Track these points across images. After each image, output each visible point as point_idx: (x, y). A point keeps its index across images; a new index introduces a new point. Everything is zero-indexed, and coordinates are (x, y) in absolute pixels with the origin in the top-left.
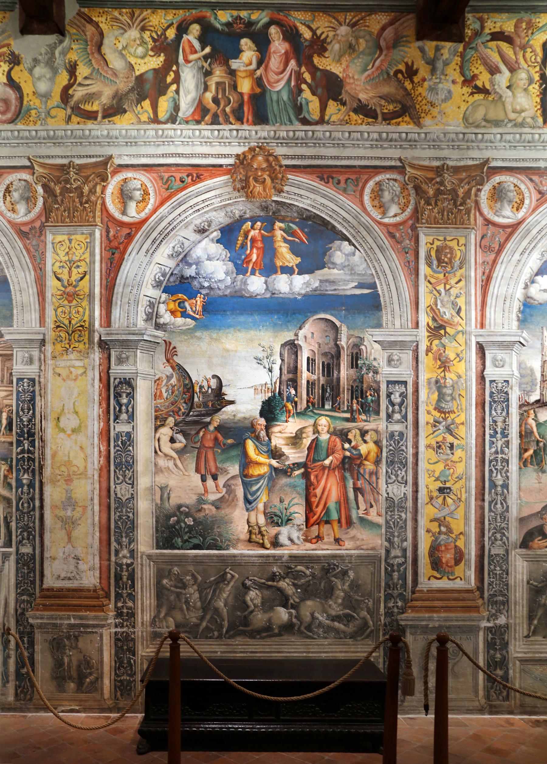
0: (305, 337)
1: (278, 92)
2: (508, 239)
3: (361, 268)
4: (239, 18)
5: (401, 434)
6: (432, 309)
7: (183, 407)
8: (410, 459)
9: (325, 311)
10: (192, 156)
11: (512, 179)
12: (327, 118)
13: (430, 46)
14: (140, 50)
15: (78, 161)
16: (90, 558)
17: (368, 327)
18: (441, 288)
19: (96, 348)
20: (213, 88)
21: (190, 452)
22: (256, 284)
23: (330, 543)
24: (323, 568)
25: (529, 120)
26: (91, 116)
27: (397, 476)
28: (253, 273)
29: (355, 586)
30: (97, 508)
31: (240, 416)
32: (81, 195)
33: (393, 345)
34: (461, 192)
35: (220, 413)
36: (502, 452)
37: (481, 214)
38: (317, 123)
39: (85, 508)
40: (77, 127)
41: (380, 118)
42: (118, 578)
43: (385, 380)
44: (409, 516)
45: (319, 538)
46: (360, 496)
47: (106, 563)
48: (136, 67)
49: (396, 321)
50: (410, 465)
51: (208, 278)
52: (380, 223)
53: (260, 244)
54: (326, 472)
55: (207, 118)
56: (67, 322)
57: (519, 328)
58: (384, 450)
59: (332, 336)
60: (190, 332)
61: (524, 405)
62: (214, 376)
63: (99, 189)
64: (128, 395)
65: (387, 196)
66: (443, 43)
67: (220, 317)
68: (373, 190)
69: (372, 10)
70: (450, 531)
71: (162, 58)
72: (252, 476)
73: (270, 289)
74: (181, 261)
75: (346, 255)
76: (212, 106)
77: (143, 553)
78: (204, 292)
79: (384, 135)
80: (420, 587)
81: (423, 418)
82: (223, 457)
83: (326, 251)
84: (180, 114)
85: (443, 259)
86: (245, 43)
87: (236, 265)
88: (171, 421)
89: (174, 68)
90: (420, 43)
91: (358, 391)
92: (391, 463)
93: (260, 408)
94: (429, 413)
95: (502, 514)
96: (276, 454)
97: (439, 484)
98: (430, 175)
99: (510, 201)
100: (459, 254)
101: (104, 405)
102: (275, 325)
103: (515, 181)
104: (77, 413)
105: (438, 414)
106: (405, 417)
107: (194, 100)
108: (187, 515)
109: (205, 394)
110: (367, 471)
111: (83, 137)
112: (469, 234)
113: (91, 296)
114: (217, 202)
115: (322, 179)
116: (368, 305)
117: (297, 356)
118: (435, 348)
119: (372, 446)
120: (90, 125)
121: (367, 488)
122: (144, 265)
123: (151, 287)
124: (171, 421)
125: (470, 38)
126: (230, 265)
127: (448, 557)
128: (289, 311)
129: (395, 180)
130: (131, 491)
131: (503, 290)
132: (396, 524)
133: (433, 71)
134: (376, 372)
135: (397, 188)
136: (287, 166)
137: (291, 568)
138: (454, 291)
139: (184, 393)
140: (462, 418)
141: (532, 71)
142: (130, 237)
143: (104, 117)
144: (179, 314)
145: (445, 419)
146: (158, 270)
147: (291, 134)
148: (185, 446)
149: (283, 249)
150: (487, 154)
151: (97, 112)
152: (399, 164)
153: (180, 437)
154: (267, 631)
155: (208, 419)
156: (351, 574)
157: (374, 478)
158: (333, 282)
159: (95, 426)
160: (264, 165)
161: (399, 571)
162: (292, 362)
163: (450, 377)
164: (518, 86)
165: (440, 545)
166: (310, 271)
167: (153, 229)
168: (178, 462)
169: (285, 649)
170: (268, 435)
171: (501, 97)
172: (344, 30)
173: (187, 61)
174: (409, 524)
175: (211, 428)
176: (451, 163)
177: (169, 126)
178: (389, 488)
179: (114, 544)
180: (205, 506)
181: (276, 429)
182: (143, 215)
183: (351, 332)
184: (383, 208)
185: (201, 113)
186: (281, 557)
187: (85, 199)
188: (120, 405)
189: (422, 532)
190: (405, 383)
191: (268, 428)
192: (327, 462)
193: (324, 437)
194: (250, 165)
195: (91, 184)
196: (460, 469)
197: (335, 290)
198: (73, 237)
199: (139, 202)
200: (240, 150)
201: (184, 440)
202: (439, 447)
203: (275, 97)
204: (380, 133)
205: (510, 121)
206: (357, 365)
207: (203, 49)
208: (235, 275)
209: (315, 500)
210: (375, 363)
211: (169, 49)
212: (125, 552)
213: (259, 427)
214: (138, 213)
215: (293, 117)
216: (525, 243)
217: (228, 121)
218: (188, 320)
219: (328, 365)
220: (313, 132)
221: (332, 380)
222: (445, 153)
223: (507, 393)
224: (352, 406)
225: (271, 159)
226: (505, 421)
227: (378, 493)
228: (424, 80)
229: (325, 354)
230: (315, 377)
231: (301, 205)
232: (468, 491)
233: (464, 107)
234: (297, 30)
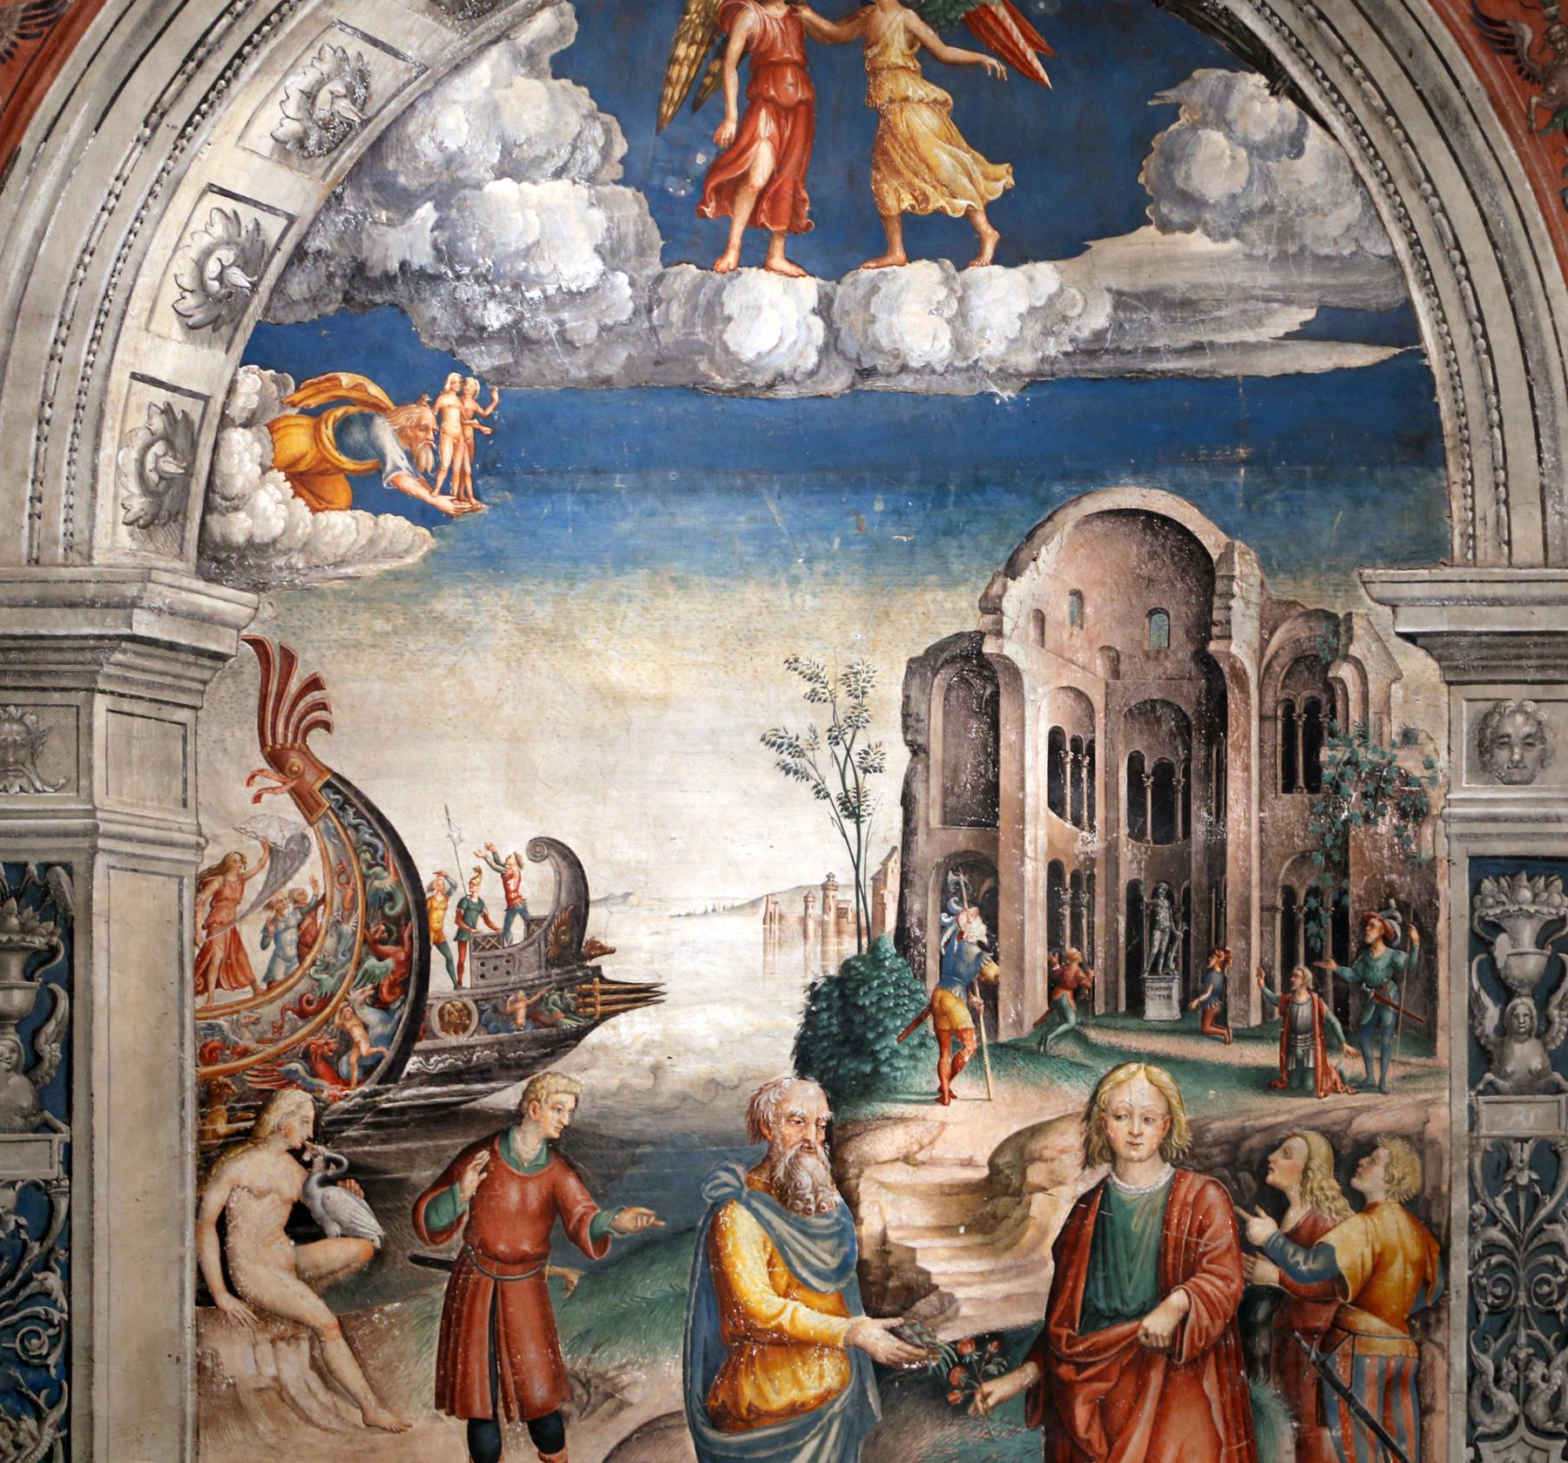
0: (1040, 618)
3: (1334, 223)
9: (1145, 470)
17: (1370, 559)
22: (772, 318)
27: (1524, 1393)
28: (754, 256)
31: (686, 1071)
35: (577, 1056)
43: (1460, 852)
51: (507, 282)
53: (790, 89)
54: (1156, 1379)
58: (1461, 1246)
59: (1179, 605)
62: (546, 847)
67: (570, 505)
72: (756, 1417)
73: (850, 346)
74: (354, 176)
75: (1258, 151)
78: (482, 359)
83: (1147, 128)
91: (1319, 922)
92: (1493, 1321)
96: (883, 1285)
102: (876, 551)
110: (1371, 1367)
117: (995, 726)
119: (1393, 1224)
122: (134, 197)
123: (176, 331)
126: (631, 206)
128: (942, 469)
134: (1415, 812)
144: (343, 493)
146: (219, 230)
149: (920, 115)
157: (1405, 1411)
158: (1184, 306)
162: (969, 758)
166: (1063, 245)
170: (840, 1180)
175: (527, 1144)
181: (883, 1144)
191: (837, 1139)
192: (1159, 1323)
193: (1144, 1179)
197: (1197, 348)
206: (1313, 770)
208: (655, 267)
210: (1409, 762)
213: (791, 1132)
218: (394, 524)
219: (1164, 771)
221: (1183, 861)
224: (1287, 1005)
229: (1145, 713)
230: (1094, 843)
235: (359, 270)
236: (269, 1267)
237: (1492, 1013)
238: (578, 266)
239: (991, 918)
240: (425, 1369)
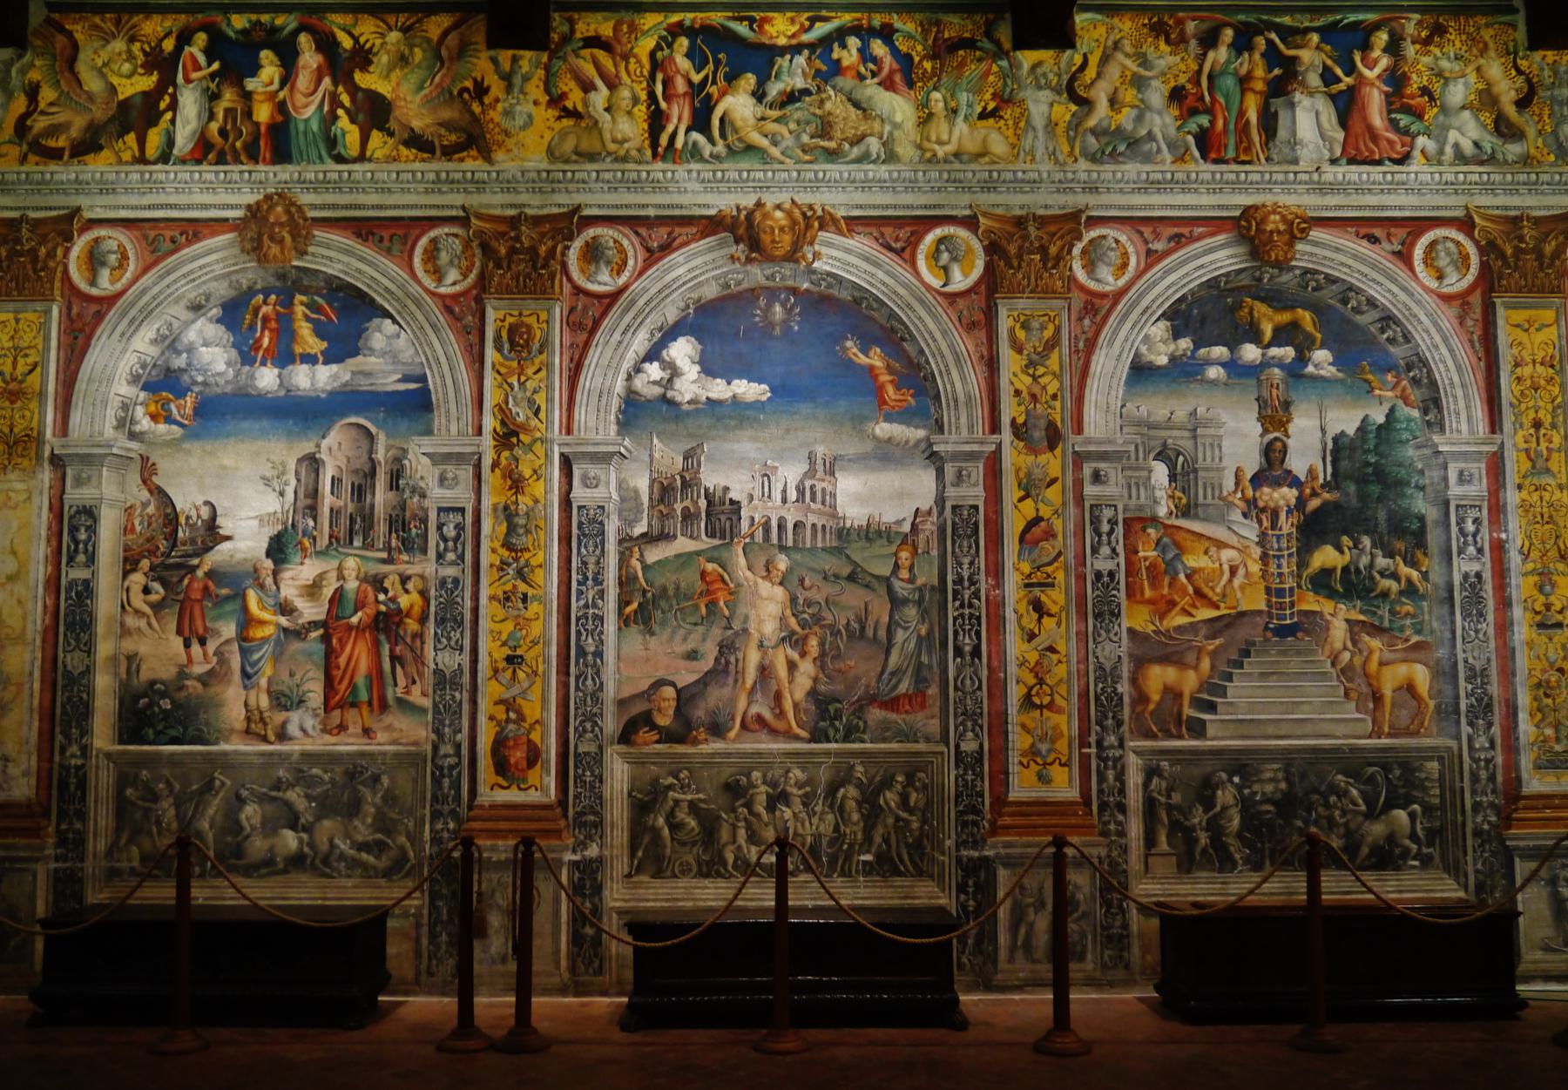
1: (307, 121)
2: (604, 314)
3: (407, 354)
4: (259, 22)
5: (456, 581)
6: (502, 411)
7: (163, 545)
8: (468, 616)
9: (357, 412)
10: (189, 207)
11: (611, 232)
12: (368, 154)
13: (505, 56)
14: (127, 67)
15: (33, 215)
16: (24, 757)
18: (514, 380)
19: (46, 465)
20: (221, 116)
21: (170, 607)
22: (267, 378)
23: (356, 735)
24: (347, 772)
25: (634, 153)
26: (55, 155)
27: (449, 639)
28: (263, 364)
29: (390, 798)
30: (37, 686)
31: (239, 556)
32: (35, 259)
33: (447, 458)
34: (543, 250)
36: (595, 606)
37: (570, 279)
38: (355, 161)
39: (20, 686)
40: (35, 168)
41: (438, 153)
42: (63, 785)
44: (466, 695)
45: (342, 728)
46: (399, 668)
47: (46, 765)
48: (119, 90)
49: (451, 425)
50: (467, 624)
51: (204, 371)
52: (433, 294)
53: (273, 325)
55: (210, 156)
56: (7, 430)
57: (619, 433)
58: (433, 603)
59: (366, 447)
60: (175, 443)
61: (625, 541)
62: (207, 503)
63: (60, 252)
64: (88, 528)
65: (444, 257)
66: (522, 52)
68: (426, 251)
69: (431, 10)
70: (521, 718)
71: (155, 77)
72: (252, 640)
74: (168, 347)
76: (218, 140)
77: (99, 751)
78: (196, 389)
79: (444, 175)
80: (480, 800)
81: (486, 558)
82: (215, 613)
83: (360, 332)
84: (175, 152)
85: (518, 341)
86: (266, 55)
87: (241, 352)
88: (145, 564)
89: (171, 90)
90: (492, 53)
91: (398, 522)
92: (441, 622)
93: (265, 545)
94: (494, 551)
95: (593, 695)
96: (285, 609)
97: (507, 651)
98: (502, 228)
99: (608, 262)
100: (538, 333)
101: (54, 543)
102: (289, 433)
103: (616, 235)
104: (14, 553)
105: (506, 553)
106: (462, 557)
107: (195, 132)
108: (163, 695)
109: (192, 527)
111: (42, 182)
112: (553, 307)
113: (42, 395)
114: (219, 269)
115: (358, 235)
116: (415, 404)
118: (503, 462)
119: (415, 597)
120: (53, 167)
121: (409, 655)
124: (145, 564)
125: (557, 45)
126: (234, 353)
127: (518, 755)
129: (456, 236)
130: (86, 661)
131: (598, 381)
132: (447, 707)
133: (509, 89)
134: (423, 496)
135: (457, 245)
136: (314, 219)
137: (302, 771)
138: (530, 385)
139: (165, 526)
140: (540, 558)
141: (637, 88)
142: (99, 317)
143: (72, 156)
145: (516, 559)
147: (321, 176)
148: (164, 599)
150: (577, 199)
151: (62, 150)
152: (461, 213)
153: (156, 586)
154: (267, 866)
155: (195, 561)
156: (385, 780)
157: (418, 643)
158: (368, 374)
159: (39, 572)
160: (284, 218)
161: (451, 776)
162: (311, 482)
163: (524, 502)
164: (619, 108)
165: (506, 738)
167: (132, 304)
168: (153, 621)
169: (293, 893)
170: (276, 583)
171: (596, 122)
172: (394, 36)
173: (188, 81)
174: (466, 707)
175: (200, 573)
176: (530, 212)
177: (159, 167)
178: (440, 657)
179: (59, 738)
180: (188, 683)
181: (287, 575)
182: (119, 286)
183: (391, 442)
184: (438, 274)
185: (203, 150)
186: (288, 755)
187: (40, 265)
188: (77, 543)
189: (482, 719)
190: (462, 510)
192: (355, 620)
193: (352, 585)
194: (265, 218)
195: (50, 245)
196: (536, 629)
198: (21, 316)
199: (114, 269)
200: (251, 199)
201: (161, 591)
202: (507, 599)
203: (301, 127)
204: (438, 173)
205: (609, 154)
207: (209, 65)
209: (338, 674)
210: (422, 484)
211: (164, 65)
212: (74, 749)
214: (112, 283)
215: (324, 153)
216: (628, 318)
217: (237, 161)
218: (174, 427)
219: (360, 486)
220: (350, 173)
222: (524, 198)
223: (602, 523)
225: (293, 209)
226: (598, 563)
227: (423, 664)
228: (497, 100)
229: (356, 472)
230: (342, 503)
231: (330, 271)
232: (547, 661)
233: (548, 137)
234: (334, 37)
235: (168, 370)
236: (138, 601)
237: (442, 546)
238: (221, 367)
239: (315, 520)
240: (173, 626)
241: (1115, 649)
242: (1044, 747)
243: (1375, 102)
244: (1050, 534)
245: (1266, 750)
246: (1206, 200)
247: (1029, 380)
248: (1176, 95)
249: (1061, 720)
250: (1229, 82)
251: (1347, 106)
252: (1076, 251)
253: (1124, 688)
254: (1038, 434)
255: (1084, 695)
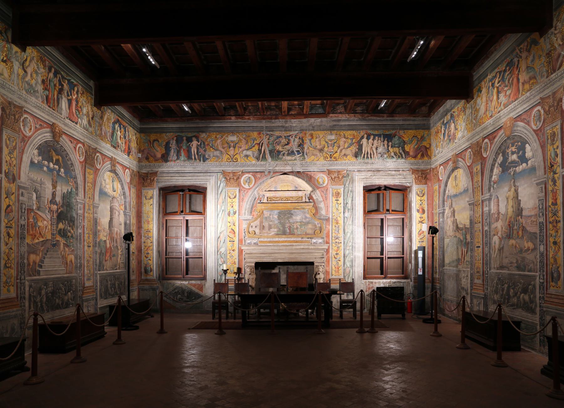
241: (24, 249)
242: (9, 281)
243: (74, 103)
244: (12, 211)
245: (50, 278)
246: (47, 117)
247: (9, 158)
248: (43, 82)
249: (12, 271)
250: (52, 84)
251: (70, 102)
252: (21, 120)
253: (26, 261)
254: (11, 177)
255: (18, 263)
